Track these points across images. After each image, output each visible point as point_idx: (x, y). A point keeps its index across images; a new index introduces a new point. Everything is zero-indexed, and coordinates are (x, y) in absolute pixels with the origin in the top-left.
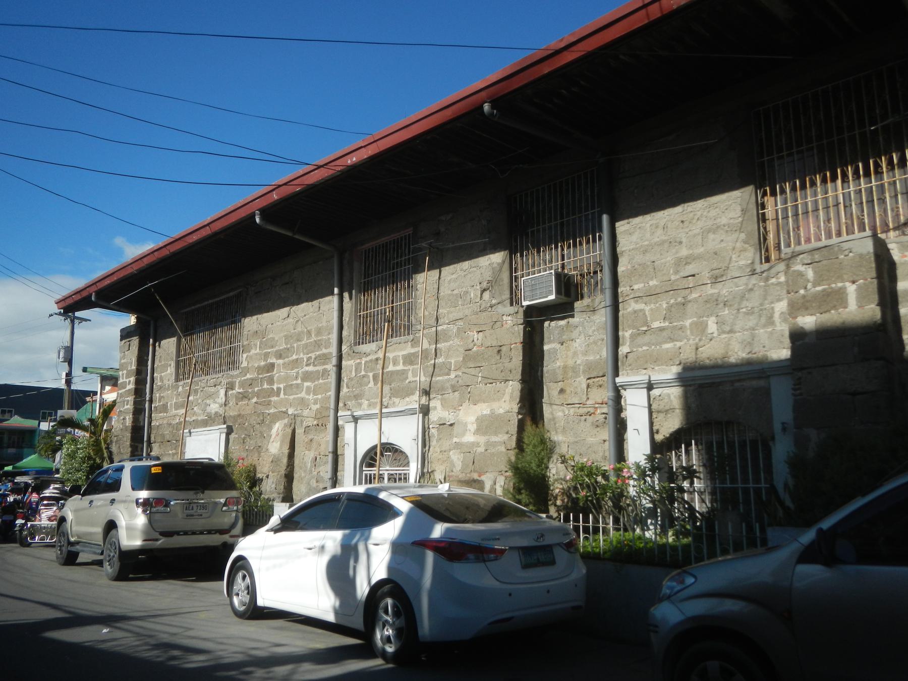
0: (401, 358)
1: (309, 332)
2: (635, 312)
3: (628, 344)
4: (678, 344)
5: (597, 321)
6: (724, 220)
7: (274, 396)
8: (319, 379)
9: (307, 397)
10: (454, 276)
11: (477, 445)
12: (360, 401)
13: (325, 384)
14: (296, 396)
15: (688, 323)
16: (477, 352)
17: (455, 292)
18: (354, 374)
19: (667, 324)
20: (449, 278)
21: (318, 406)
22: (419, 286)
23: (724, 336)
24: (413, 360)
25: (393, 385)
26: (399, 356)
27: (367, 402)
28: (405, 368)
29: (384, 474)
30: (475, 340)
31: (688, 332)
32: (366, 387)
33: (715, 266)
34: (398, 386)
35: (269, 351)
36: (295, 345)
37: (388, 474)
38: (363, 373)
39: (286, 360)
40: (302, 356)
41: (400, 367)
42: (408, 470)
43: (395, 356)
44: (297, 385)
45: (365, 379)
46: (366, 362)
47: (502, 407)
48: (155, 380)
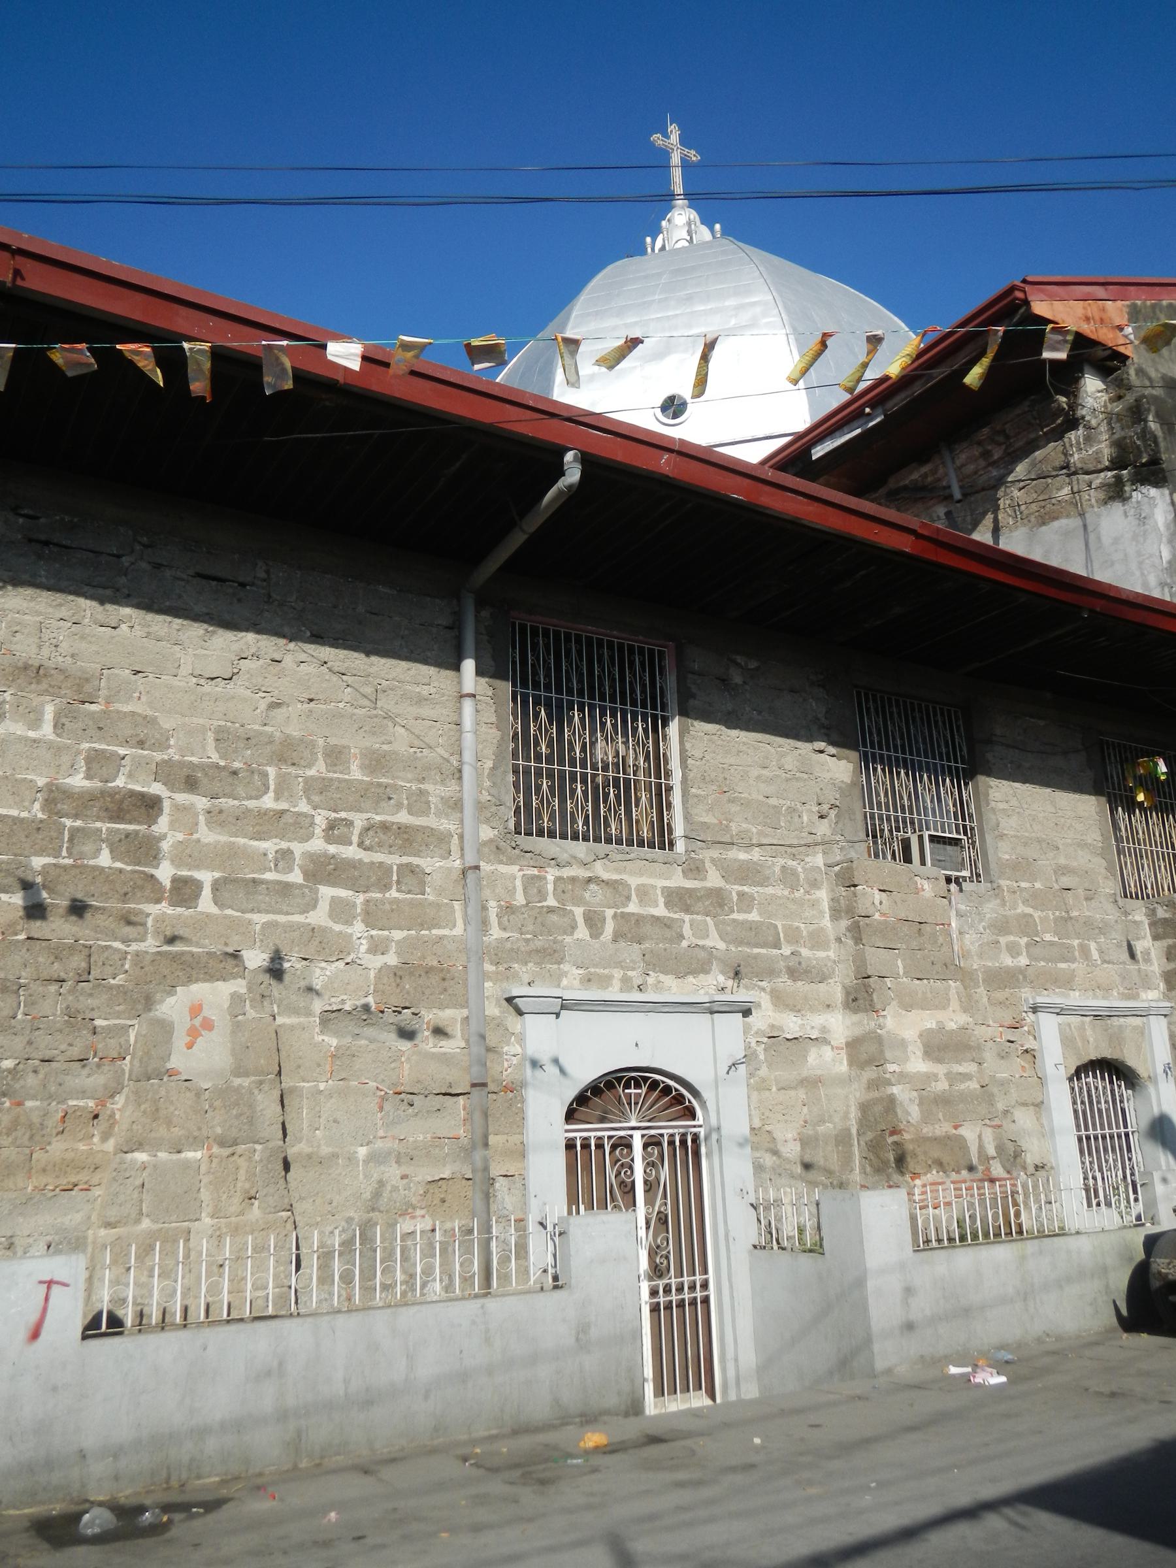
0: (659, 892)
1: (336, 756)
2: (1025, 915)
3: (1024, 954)
4: (1073, 966)
5: (988, 916)
6: (1089, 841)
7: (158, 901)
8: (387, 887)
9: (337, 928)
10: (765, 772)
11: (934, 1077)
12: (556, 966)
13: (411, 903)
14: (281, 919)
15: (1076, 942)
16: (880, 922)
17: (773, 801)
18: (520, 899)
19: (1056, 939)
20: (756, 774)
21: (392, 959)
22: (690, 761)
23: (1106, 965)
24: (689, 902)
25: (646, 945)
26: (654, 887)
27: (581, 971)
28: (672, 915)
29: (631, 1136)
30: (877, 902)
31: (1077, 953)
32: (568, 939)
33: (1086, 885)
34: (665, 950)
35: (122, 751)
36: (271, 771)
37: (643, 1136)
38: (551, 902)
39: (226, 803)
40: (303, 807)
41: (660, 911)
42: (567, 1131)
43: (643, 885)
44: (285, 889)
45: (554, 918)
46: (558, 880)
47: (952, 1020)
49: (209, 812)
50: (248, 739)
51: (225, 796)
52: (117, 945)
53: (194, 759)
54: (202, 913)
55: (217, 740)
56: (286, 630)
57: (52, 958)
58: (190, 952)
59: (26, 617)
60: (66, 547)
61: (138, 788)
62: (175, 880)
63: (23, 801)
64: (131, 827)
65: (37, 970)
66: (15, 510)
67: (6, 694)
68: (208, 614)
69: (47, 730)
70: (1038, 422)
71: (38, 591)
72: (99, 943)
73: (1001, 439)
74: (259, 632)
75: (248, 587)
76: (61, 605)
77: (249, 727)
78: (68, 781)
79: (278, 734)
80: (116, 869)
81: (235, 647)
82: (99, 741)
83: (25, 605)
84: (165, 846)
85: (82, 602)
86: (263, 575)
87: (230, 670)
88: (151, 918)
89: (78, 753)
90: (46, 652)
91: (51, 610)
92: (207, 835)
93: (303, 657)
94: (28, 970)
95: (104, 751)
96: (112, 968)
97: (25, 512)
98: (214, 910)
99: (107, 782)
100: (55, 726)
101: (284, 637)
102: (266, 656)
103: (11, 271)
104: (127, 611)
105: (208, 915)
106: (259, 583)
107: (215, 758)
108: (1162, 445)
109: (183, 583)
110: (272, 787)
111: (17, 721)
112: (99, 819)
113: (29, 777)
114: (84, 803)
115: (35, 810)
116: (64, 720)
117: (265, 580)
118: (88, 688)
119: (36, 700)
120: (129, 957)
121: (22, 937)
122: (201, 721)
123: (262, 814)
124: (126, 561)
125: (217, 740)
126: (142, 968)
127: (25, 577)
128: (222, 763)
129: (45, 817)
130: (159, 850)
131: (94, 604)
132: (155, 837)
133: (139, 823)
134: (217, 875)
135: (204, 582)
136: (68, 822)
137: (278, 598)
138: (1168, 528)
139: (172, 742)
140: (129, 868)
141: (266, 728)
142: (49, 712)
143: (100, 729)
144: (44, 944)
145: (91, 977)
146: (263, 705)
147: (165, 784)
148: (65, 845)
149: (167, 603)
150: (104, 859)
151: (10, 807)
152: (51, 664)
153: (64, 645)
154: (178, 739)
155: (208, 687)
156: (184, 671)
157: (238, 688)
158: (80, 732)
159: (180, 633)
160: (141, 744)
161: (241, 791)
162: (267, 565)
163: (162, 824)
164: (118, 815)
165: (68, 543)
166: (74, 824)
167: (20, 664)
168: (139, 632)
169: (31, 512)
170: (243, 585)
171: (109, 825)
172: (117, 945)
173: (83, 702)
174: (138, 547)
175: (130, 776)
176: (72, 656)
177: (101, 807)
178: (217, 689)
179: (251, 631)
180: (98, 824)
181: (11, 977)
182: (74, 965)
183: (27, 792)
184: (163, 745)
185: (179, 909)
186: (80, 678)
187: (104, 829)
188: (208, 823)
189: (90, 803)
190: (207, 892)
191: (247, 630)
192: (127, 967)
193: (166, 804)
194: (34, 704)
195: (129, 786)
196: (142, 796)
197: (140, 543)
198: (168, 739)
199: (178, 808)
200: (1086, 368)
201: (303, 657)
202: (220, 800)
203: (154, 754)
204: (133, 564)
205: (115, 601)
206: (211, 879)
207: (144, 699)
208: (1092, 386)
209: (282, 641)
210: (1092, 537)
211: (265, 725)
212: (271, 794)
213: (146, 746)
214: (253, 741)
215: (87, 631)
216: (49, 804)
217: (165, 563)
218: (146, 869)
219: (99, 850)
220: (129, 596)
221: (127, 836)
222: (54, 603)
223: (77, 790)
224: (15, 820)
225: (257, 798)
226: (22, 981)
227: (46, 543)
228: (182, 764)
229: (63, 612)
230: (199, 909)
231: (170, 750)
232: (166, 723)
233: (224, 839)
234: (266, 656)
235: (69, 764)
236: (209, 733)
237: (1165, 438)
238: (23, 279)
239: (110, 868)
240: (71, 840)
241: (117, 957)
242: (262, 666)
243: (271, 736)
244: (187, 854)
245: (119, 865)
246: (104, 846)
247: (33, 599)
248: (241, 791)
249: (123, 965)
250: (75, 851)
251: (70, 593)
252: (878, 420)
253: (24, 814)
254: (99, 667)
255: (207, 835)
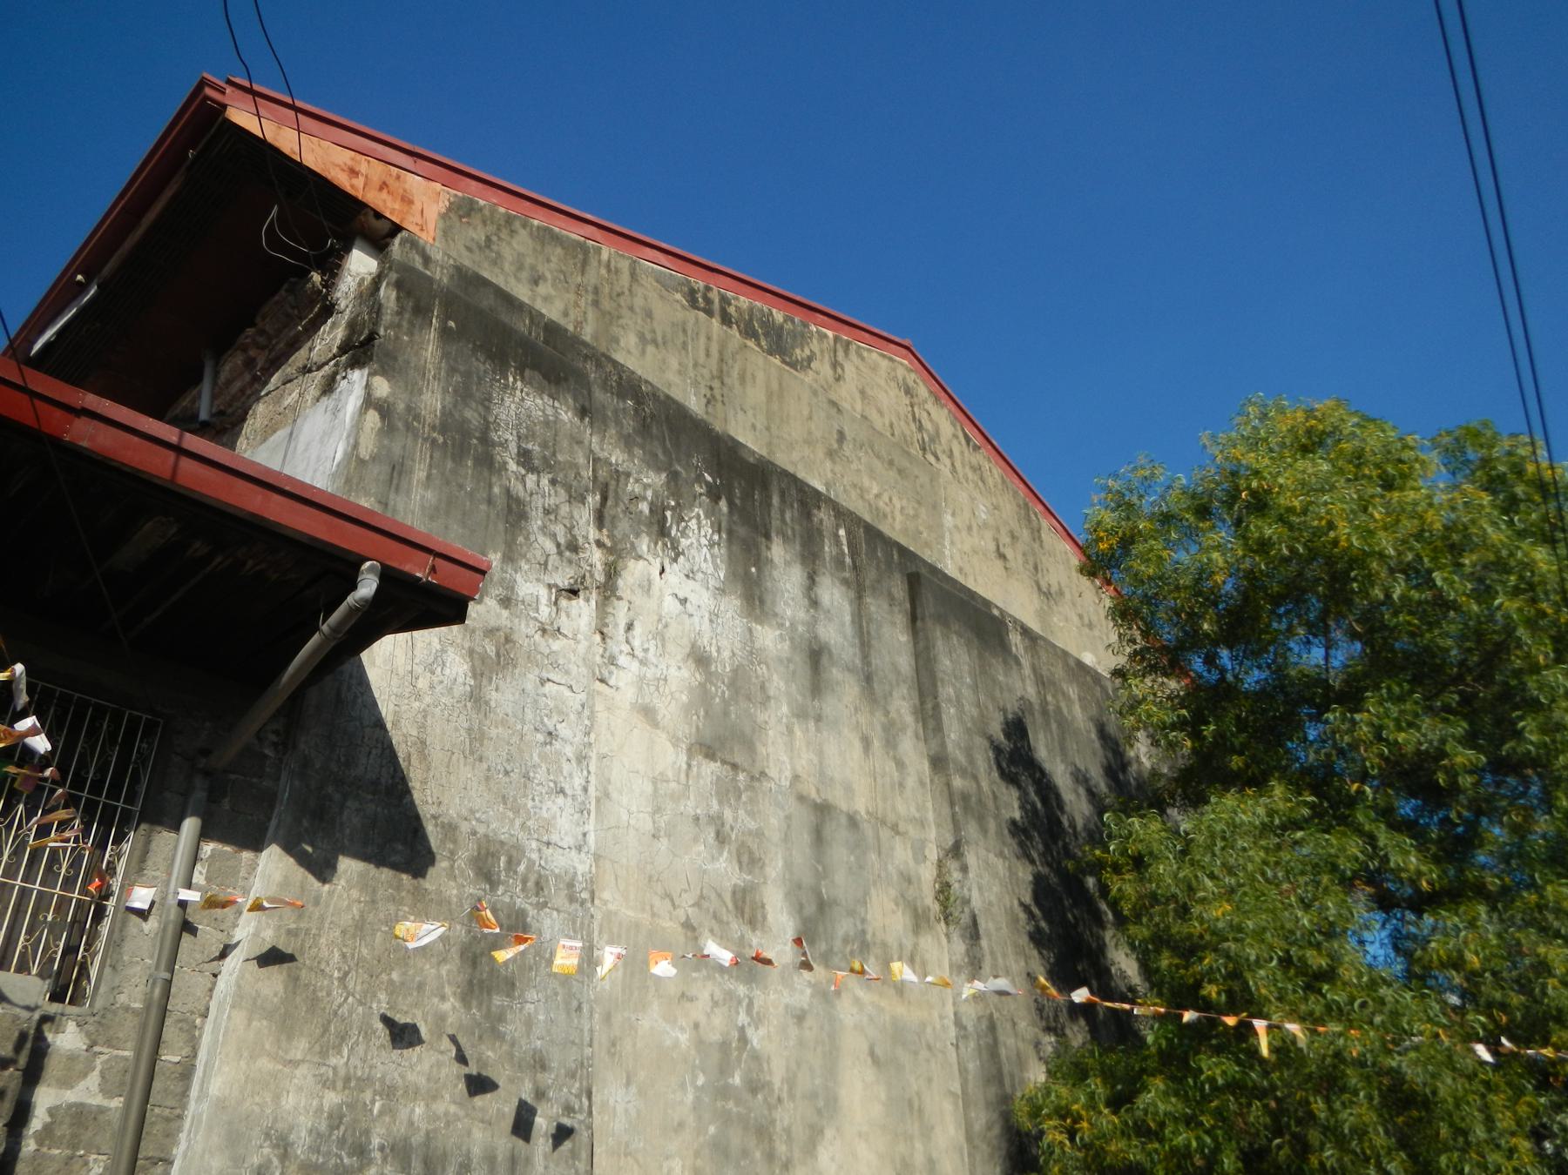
70: (296, 312)
73: (261, 340)
108: (387, 317)
138: (352, 419)
200: (358, 242)
208: (360, 264)
210: (292, 445)
237: (400, 313)
252: (92, 292)
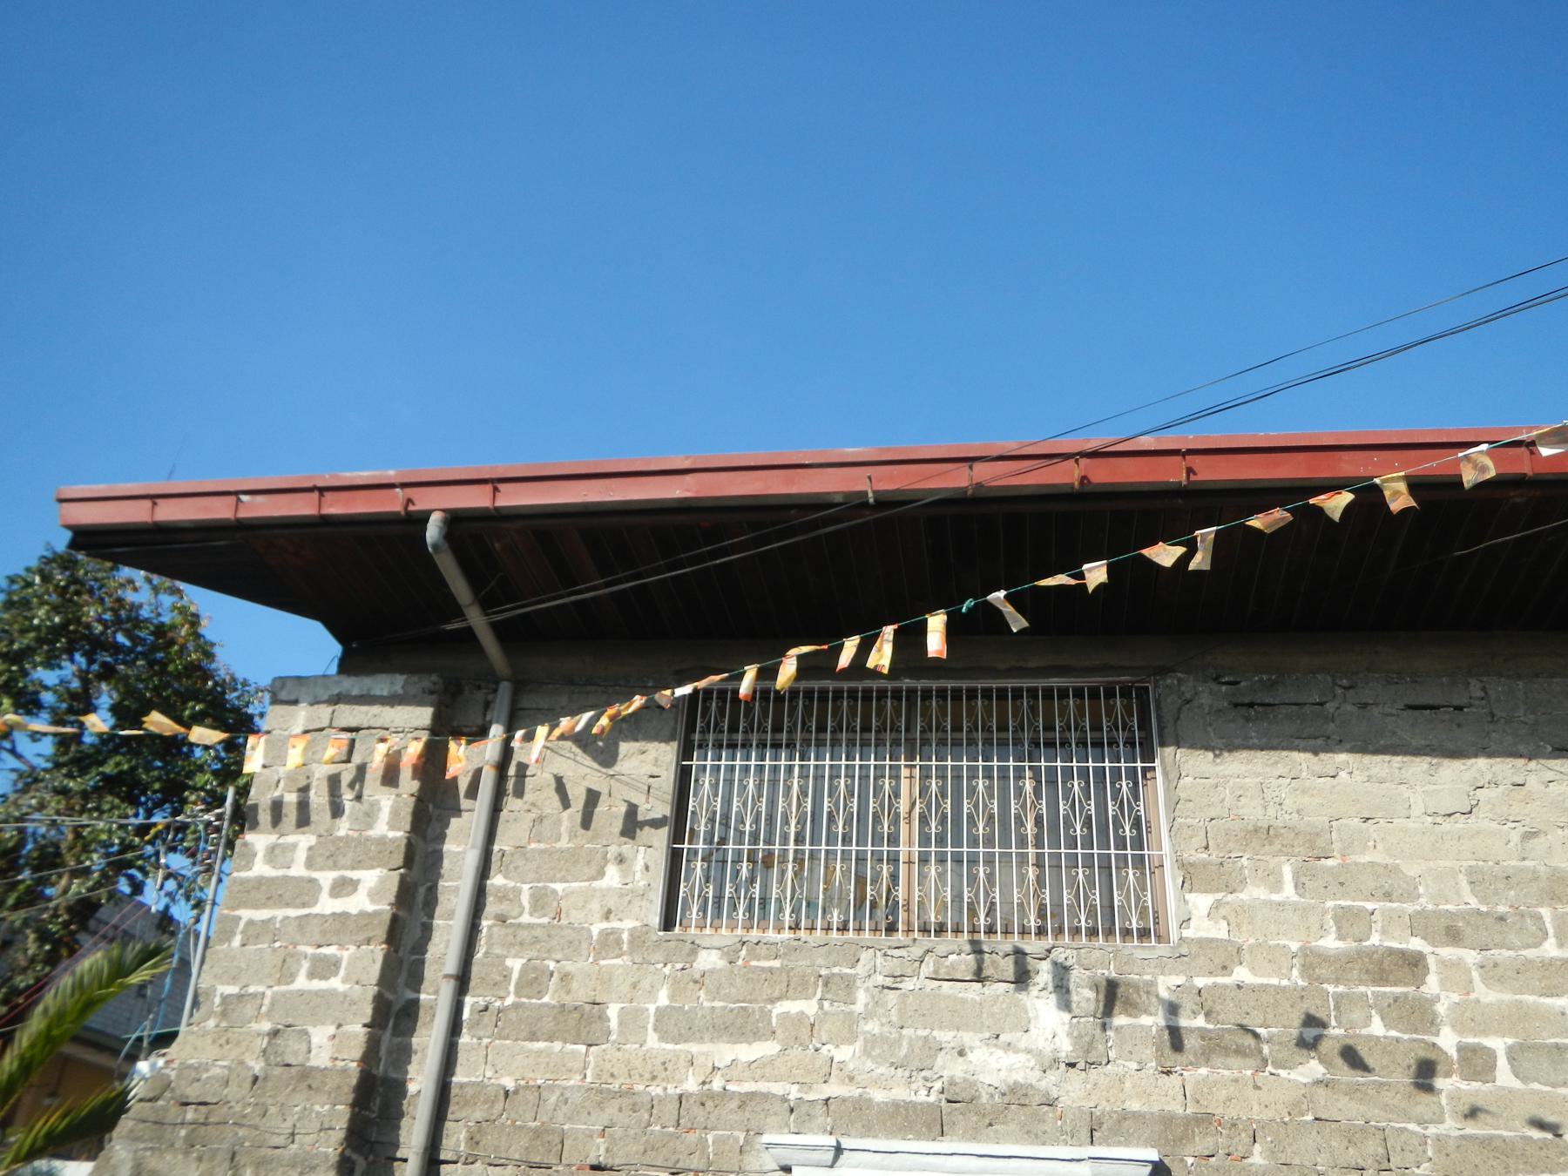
35: (1370, 906)
36: (1545, 912)
48: (490, 899)
49: (1482, 967)
50: (1507, 878)
51: (1496, 946)
52: (1412, 1126)
53: (1450, 907)
54: (1503, 1088)
55: (1472, 883)
56: (1521, 748)
57: (1345, 1143)
58: (1500, 1136)
59: (1247, 780)
60: (1270, 705)
61: (1395, 945)
62: (1461, 1049)
63: (1280, 968)
64: (1398, 990)
65: (1332, 1155)
66: (1216, 679)
67: (1243, 859)
68: (1428, 746)
69: (1289, 892)
71: (1252, 752)
72: (1392, 1124)
74: (1490, 755)
75: (1465, 710)
76: (1276, 763)
77: (1505, 864)
78: (1321, 943)
79: (1543, 868)
80: (1393, 1038)
81: (1467, 776)
82: (1343, 897)
83: (1243, 768)
84: (1441, 1008)
85: (1295, 755)
86: (1481, 694)
87: (1467, 802)
88: (1444, 1094)
89: (1325, 912)
90: (1271, 811)
91: (1268, 769)
92: (1487, 995)
93: (1550, 775)
94: (1323, 1155)
95: (1350, 908)
96: (1414, 1155)
97: (1227, 679)
98: (1517, 1084)
99: (1361, 940)
100: (1296, 886)
101: (1521, 756)
102: (1505, 782)
103: (1184, 471)
104: (1342, 757)
105: (1511, 1091)
106: (1477, 702)
107: (1474, 903)
109: (1393, 718)
110: (1551, 931)
111: (1259, 886)
112: (1361, 982)
113: (1282, 942)
114: (1342, 966)
115: (1294, 977)
116: (1303, 879)
117: (1482, 699)
118: (1320, 843)
119: (1273, 862)
120: (1429, 1141)
121: (1309, 1117)
122: (1448, 864)
123: (1547, 964)
124: (1330, 707)
125: (1472, 883)
126: (1447, 1155)
127: (1238, 741)
128: (1484, 909)
129: (1306, 984)
130: (1435, 1014)
131: (1309, 756)
132: (1427, 1000)
133: (1406, 984)
134: (1510, 1041)
135: (1416, 713)
136: (1331, 988)
137: (1503, 714)
139: (1421, 890)
140: (1406, 1037)
141: (1527, 863)
142: (1287, 872)
143: (1342, 884)
144: (1334, 1125)
145: (1392, 1165)
146: (1515, 837)
147: (1424, 938)
148: (1333, 1014)
149: (1382, 742)
150: (1377, 1028)
151: (1269, 975)
152: (1279, 823)
153: (1287, 802)
154: (1427, 885)
155: (1447, 825)
156: (1417, 810)
157: (1481, 821)
158: (1322, 890)
159: (1403, 771)
160: (1388, 896)
161: (1513, 938)
162: (1481, 681)
163: (1432, 985)
164: (1381, 978)
165: (1271, 700)
166: (1336, 990)
167: (1250, 828)
168: (1359, 777)
169: (1232, 679)
170: (1459, 708)
171: (1373, 989)
172: (1412, 1126)
173: (1319, 858)
174: (1339, 691)
175: (1384, 932)
176: (1298, 812)
177: (1361, 970)
178: (1458, 825)
179: (1480, 756)
180: (1362, 989)
181: (1308, 1164)
182: (1371, 1150)
183: (1283, 959)
184: (1412, 895)
185: (1474, 1084)
186: (1310, 834)
187: (1369, 994)
188: (1484, 980)
189: (1350, 965)
190: (1502, 1062)
191: (1476, 756)
192: (1430, 1153)
193: (1431, 961)
194: (1271, 866)
195: (1387, 944)
196: (1402, 954)
197: (1340, 686)
198: (1416, 888)
199: (1444, 964)
201: (1550, 775)
202: (1492, 952)
203: (1405, 905)
204: (1338, 708)
205: (1328, 749)
206: (1503, 1046)
207: (1380, 847)
209: (1520, 762)
211: (1524, 859)
212: (1552, 940)
213: (1394, 897)
214: (1514, 880)
215: (1307, 784)
216: (1306, 969)
217: (1371, 702)
218: (1426, 1037)
219: (1370, 1017)
220: (1341, 741)
221: (1396, 1000)
222: (1270, 762)
223: (1332, 952)
224: (1279, 990)
225: (1537, 945)
226: (1319, 1168)
227: (1251, 705)
228: (1438, 914)
229: (1280, 770)
230: (1498, 1083)
231: (1421, 900)
232: (1411, 870)
233: (1508, 997)
234: (1505, 782)
235: (1318, 926)
236: (1461, 876)
238: (1195, 474)
239: (1385, 1037)
240: (1337, 1007)
241: (1416, 1141)
242: (1503, 793)
243: (1534, 872)
244: (1467, 1018)
245: (1393, 1033)
246: (1373, 1012)
247: (1249, 762)
248: (1513, 938)
249: (1425, 1152)
250: (1344, 1021)
251: (1283, 749)
253: (1285, 982)
254: (1326, 819)
255: (1487, 995)
